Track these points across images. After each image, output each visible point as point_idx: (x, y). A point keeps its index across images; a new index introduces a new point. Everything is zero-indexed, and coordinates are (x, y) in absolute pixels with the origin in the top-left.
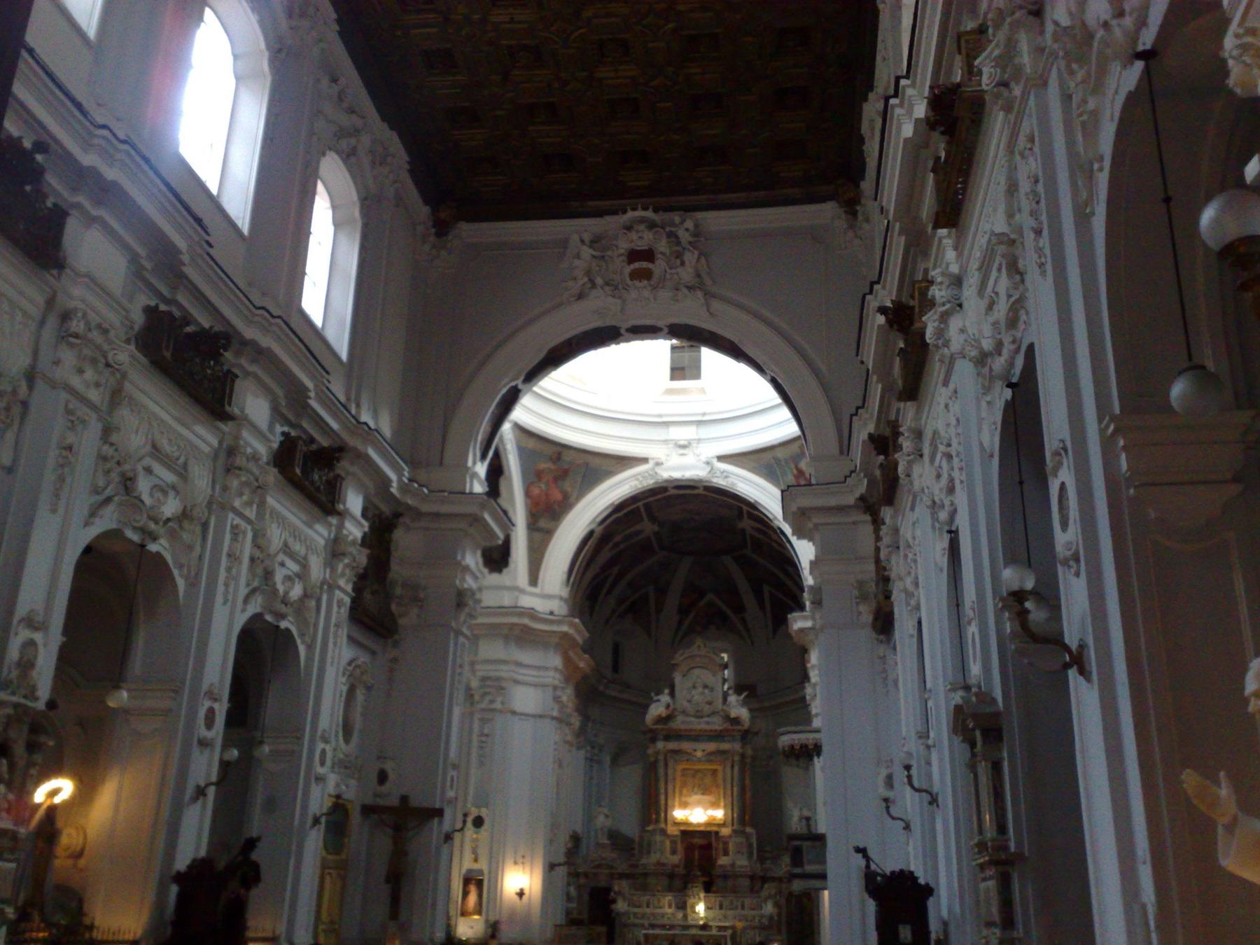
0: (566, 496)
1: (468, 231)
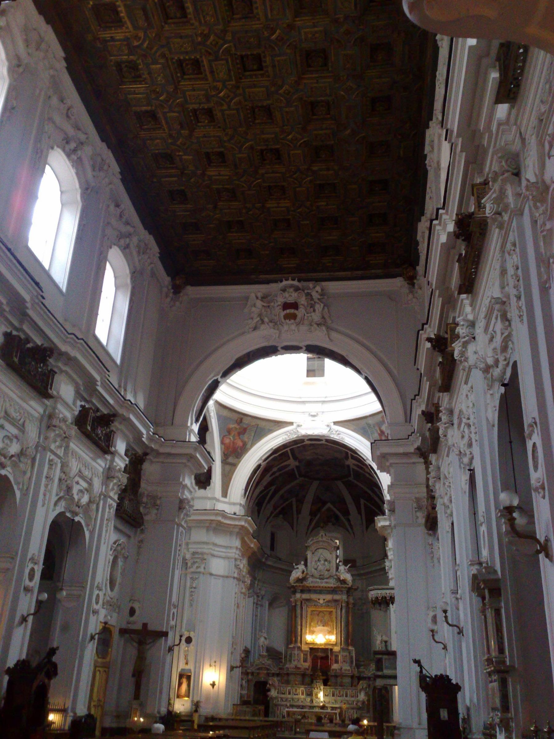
0: (245, 444)
1: (191, 291)
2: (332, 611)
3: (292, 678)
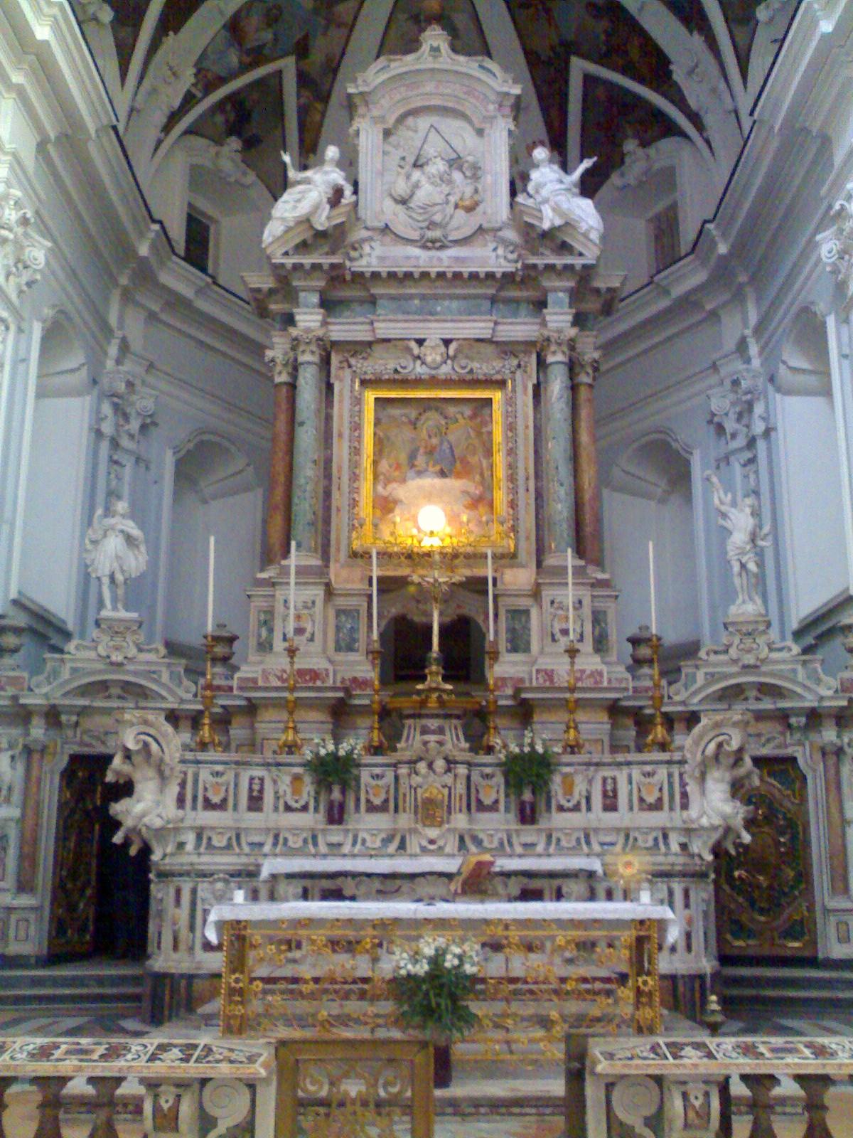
2: (489, 402)
3: (270, 725)
